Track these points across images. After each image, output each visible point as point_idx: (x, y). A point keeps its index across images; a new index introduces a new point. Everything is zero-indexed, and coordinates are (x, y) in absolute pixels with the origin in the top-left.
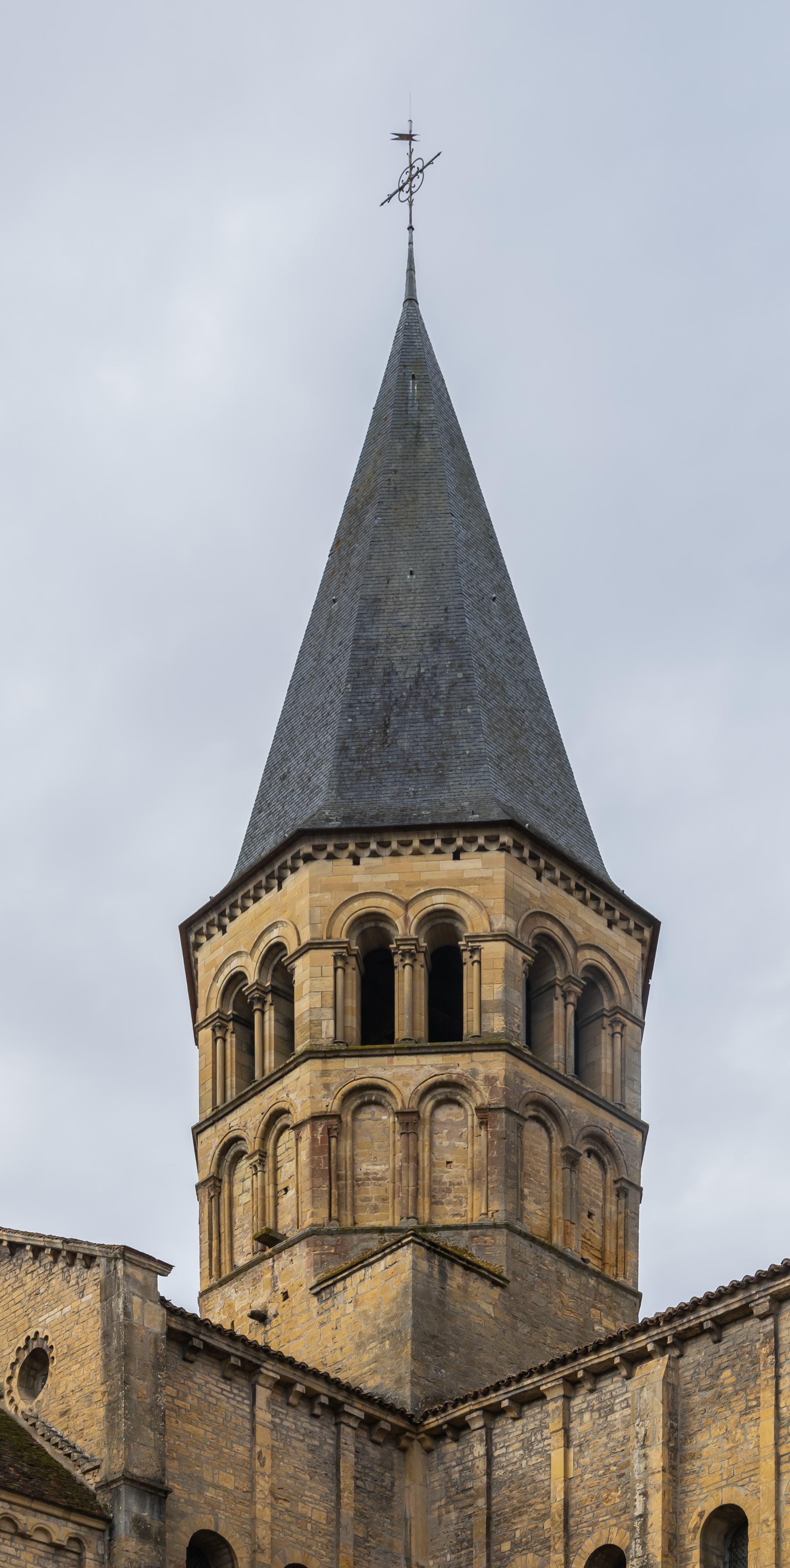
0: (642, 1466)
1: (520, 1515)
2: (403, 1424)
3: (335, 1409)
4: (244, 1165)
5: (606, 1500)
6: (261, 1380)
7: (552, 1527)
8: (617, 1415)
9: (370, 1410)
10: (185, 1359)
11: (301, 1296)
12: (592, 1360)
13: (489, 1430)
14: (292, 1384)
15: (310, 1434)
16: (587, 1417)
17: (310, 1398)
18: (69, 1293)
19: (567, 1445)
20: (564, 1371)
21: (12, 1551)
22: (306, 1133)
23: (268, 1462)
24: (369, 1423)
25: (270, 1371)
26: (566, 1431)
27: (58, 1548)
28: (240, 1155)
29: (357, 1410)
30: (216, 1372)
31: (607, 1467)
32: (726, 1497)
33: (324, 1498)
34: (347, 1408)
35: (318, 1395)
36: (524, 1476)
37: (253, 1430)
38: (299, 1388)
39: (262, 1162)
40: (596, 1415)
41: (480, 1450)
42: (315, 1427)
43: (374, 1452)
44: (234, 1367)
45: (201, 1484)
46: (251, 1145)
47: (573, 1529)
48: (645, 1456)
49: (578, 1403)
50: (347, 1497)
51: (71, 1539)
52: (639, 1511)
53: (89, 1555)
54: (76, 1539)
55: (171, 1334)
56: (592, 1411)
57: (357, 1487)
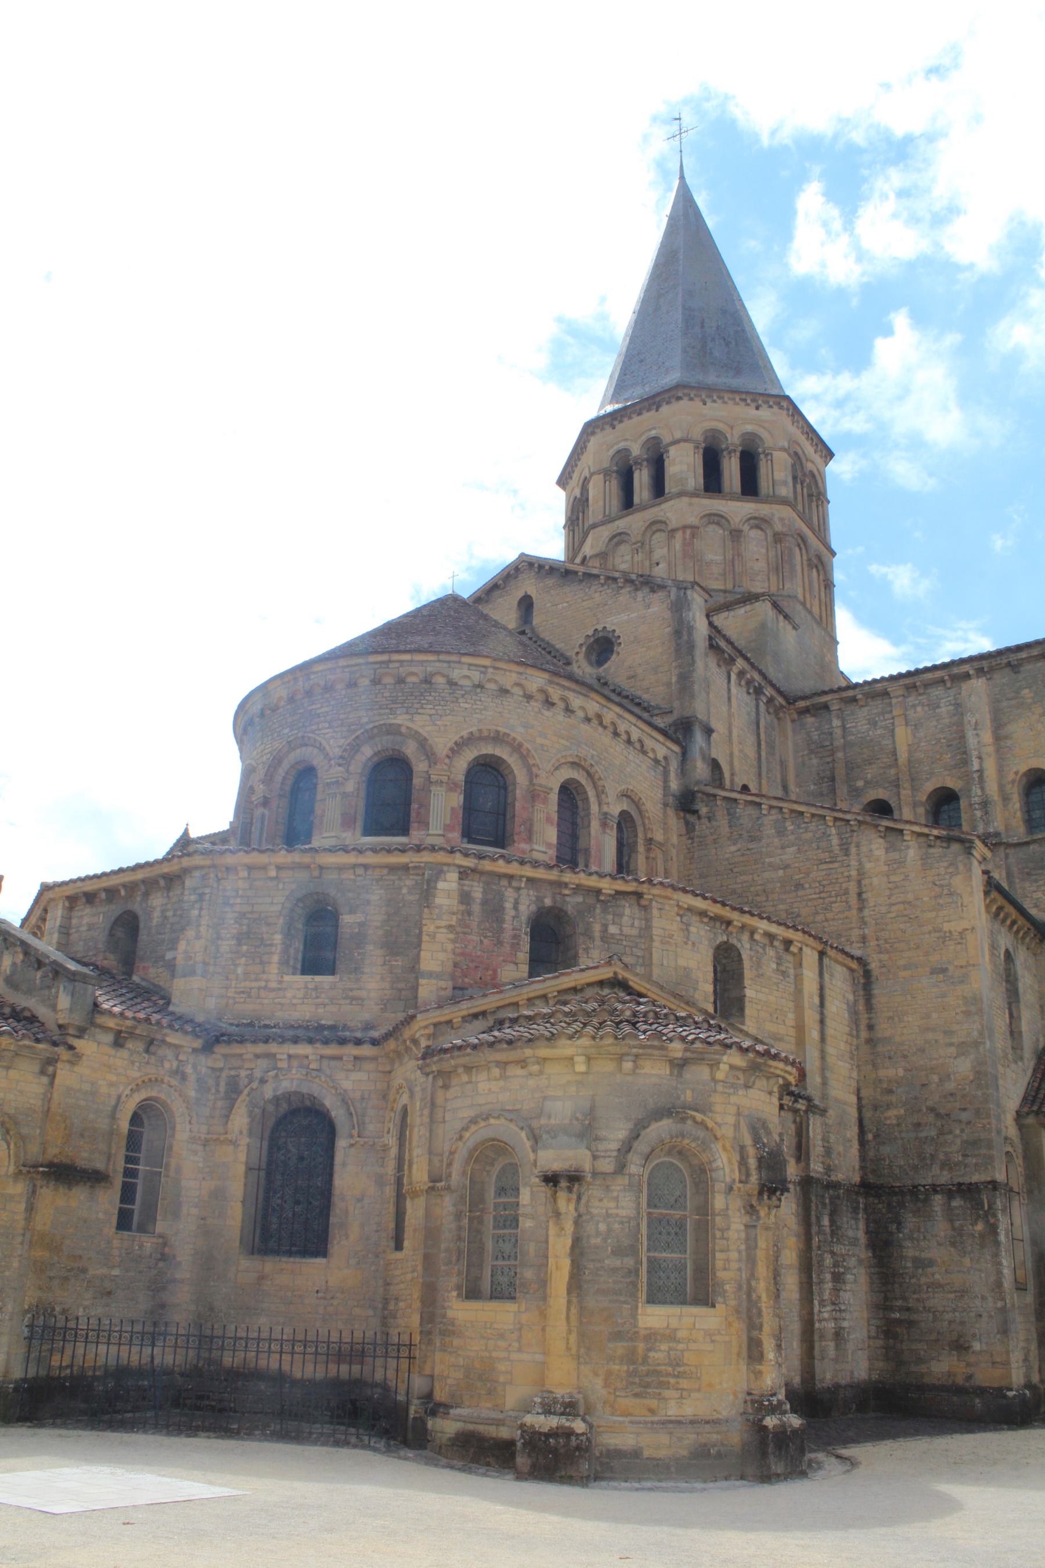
0: (976, 741)
1: (870, 764)
5: (940, 759)
8: (943, 709)
19: (907, 724)
31: (938, 740)
36: (871, 740)
38: (748, 676)
40: (926, 708)
44: (725, 659)
48: (977, 735)
52: (976, 766)
56: (923, 706)
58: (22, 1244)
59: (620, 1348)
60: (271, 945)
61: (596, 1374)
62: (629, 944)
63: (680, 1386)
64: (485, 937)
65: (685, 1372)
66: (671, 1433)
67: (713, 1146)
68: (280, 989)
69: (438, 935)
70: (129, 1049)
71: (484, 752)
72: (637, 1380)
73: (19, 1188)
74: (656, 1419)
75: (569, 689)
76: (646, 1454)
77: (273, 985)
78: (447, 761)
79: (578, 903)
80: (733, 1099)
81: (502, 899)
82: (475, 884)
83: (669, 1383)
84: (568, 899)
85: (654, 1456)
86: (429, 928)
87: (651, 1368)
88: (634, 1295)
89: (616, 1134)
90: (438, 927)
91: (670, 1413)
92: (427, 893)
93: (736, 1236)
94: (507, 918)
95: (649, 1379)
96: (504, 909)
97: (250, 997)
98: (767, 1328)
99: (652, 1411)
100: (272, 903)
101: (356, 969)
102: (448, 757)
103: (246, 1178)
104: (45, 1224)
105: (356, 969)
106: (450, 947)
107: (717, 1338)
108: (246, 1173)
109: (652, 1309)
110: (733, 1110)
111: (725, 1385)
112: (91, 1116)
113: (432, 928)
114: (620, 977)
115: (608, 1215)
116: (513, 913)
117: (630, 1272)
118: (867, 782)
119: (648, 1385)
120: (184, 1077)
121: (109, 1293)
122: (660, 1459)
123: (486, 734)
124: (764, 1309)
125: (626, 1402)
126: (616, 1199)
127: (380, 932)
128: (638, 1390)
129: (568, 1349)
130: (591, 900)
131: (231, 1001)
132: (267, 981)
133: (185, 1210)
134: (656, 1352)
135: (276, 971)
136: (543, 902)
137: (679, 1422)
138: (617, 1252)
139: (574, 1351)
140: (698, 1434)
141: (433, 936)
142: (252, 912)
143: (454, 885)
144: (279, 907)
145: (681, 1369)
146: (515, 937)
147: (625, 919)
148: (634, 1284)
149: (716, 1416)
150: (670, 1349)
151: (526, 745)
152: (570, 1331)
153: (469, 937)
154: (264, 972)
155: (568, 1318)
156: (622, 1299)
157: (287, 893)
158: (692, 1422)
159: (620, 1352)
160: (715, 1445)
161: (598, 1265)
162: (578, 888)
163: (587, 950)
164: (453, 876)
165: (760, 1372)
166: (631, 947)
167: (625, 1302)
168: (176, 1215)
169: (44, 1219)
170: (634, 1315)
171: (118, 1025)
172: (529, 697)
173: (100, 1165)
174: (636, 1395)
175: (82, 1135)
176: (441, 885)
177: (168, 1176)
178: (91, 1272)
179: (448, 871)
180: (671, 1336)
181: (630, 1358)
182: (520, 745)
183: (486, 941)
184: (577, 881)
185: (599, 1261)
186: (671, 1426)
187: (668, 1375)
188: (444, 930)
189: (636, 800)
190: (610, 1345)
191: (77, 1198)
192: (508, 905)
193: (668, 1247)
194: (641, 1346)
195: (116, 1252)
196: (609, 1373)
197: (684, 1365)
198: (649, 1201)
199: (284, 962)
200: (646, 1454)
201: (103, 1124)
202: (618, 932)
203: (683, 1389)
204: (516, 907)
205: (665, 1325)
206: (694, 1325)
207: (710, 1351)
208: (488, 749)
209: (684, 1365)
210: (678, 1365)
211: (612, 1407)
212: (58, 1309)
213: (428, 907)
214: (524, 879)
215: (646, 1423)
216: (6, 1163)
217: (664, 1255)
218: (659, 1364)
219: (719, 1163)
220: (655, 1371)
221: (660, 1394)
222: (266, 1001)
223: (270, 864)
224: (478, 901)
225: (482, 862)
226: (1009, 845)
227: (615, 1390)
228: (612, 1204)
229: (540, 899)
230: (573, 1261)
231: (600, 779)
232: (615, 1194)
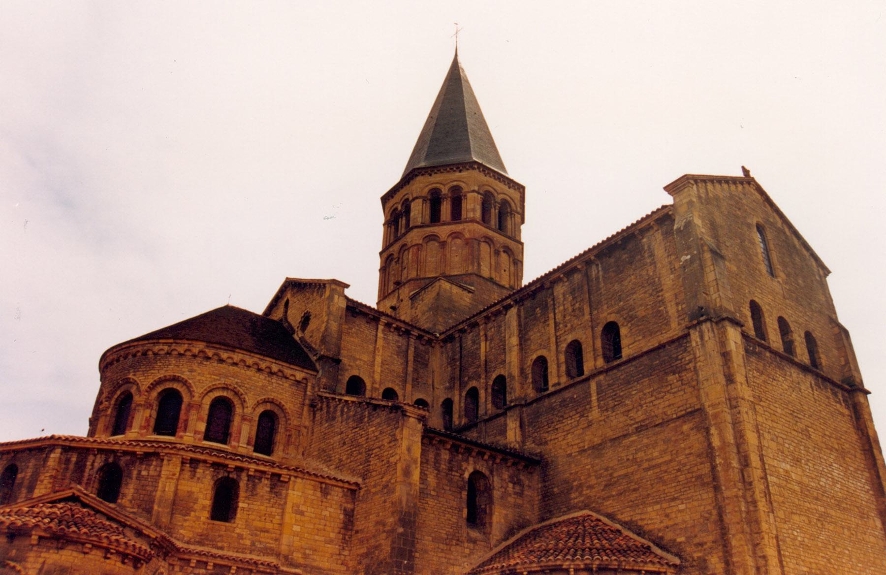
2: (433, 338)
3: (407, 333)
4: (393, 262)
6: (380, 323)
7: (481, 370)
9: (421, 333)
10: (353, 316)
11: (407, 303)
12: (493, 309)
13: (461, 338)
14: (392, 324)
15: (398, 341)
16: (493, 330)
17: (398, 329)
18: (318, 298)
20: (485, 314)
21: (280, 383)
22: (411, 250)
23: (381, 351)
24: (420, 337)
25: (383, 320)
26: (486, 336)
27: (298, 382)
28: (392, 260)
29: (415, 333)
30: (364, 321)
32: (540, 353)
33: (402, 364)
34: (412, 332)
35: (401, 328)
37: (376, 341)
39: (398, 260)
41: (458, 345)
42: (400, 339)
43: (421, 347)
44: (371, 319)
45: (355, 359)
46: (396, 256)
47: (488, 370)
49: (490, 325)
50: (411, 363)
51: (303, 379)
53: (309, 384)
54: (305, 379)
55: (348, 308)
57: (414, 360)
71: (168, 387)
75: (220, 349)
78: (146, 393)
80: (43, 555)
81: (86, 461)
92: (46, 460)
94: (87, 470)
102: (147, 391)
106: (50, 486)
110: (41, 560)
116: (90, 467)
118: (469, 378)
123: (168, 377)
127: (28, 481)
141: (42, 481)
147: (152, 467)
151: (190, 381)
163: (127, 484)
164: (59, 450)
172: (194, 356)
176: (52, 455)
182: (186, 381)
189: (278, 403)
204: (92, 465)
208: (169, 385)
224: (73, 462)
226: (522, 406)
229: (106, 460)
231: (242, 394)
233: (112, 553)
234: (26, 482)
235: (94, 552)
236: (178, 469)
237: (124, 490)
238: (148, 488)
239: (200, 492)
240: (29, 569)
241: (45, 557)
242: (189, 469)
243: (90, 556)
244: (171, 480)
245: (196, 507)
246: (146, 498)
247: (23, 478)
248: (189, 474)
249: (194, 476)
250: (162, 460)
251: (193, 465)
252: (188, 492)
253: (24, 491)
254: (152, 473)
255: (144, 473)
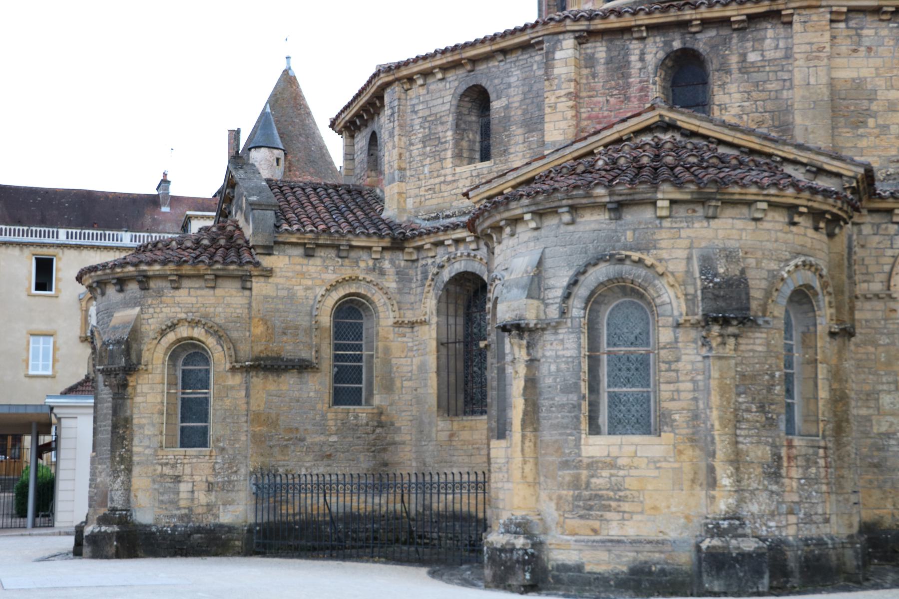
58: (246, 422)
59: (567, 475)
60: (446, 142)
61: (551, 499)
62: (773, 68)
63: (622, 509)
64: (612, 96)
65: (626, 497)
66: (609, 551)
67: (657, 282)
68: (454, 181)
69: (559, 105)
70: (321, 257)
72: (581, 503)
73: (237, 380)
74: (598, 538)
76: (588, 568)
77: (449, 178)
79: (712, 38)
80: (684, 233)
81: (627, 54)
82: (599, 44)
83: (610, 506)
84: (699, 36)
85: (595, 570)
86: (551, 99)
87: (593, 493)
88: (577, 428)
89: (558, 281)
90: (558, 97)
91: (612, 533)
92: (548, 64)
93: (689, 367)
95: (591, 503)
96: (629, 62)
97: (435, 193)
98: (720, 455)
99: (595, 531)
100: (443, 103)
101: (505, 151)
103: (438, 351)
104: (259, 406)
105: (505, 151)
107: (664, 465)
108: (438, 347)
109: (594, 439)
110: (685, 243)
111: (673, 509)
112: (291, 316)
113: (553, 99)
114: (667, 119)
115: (557, 357)
116: (639, 65)
117: (574, 407)
119: (591, 508)
120: (382, 273)
121: (329, 456)
122: (600, 574)
124: (717, 438)
125: (574, 523)
126: (562, 340)
127: (519, 112)
128: (582, 512)
129: (524, 477)
130: (725, 32)
131: (423, 199)
132: (445, 176)
133: (398, 384)
134: (598, 478)
135: (451, 165)
136: (671, 46)
137: (619, 542)
138: (566, 390)
139: (530, 479)
140: (637, 552)
141: (554, 107)
142: (430, 116)
143: (570, 52)
144: (447, 106)
145: (622, 494)
146: (642, 89)
147: (768, 41)
148: (577, 418)
149: (661, 537)
150: (612, 475)
152: (525, 462)
153: (595, 99)
154: (442, 168)
155: (523, 450)
156: (569, 431)
157: (452, 91)
158: (633, 542)
159: (568, 478)
160: (658, 563)
161: (551, 402)
162: (706, 23)
163: (723, 86)
164: (569, 42)
165: (714, 497)
166: (776, 72)
167: (571, 435)
168: (389, 387)
169: (259, 400)
170: (578, 445)
171: (299, 239)
173: (306, 354)
174: (581, 517)
175: (284, 333)
176: (558, 55)
177: (377, 358)
178: (309, 440)
179: (564, 39)
180: (612, 464)
181: (575, 484)
183: (612, 100)
184: (698, 16)
185: (553, 399)
186: (610, 544)
187: (610, 499)
188: (564, 99)
190: (560, 473)
191: (288, 383)
192: (634, 58)
193: (628, 382)
194: (584, 473)
195: (331, 423)
196: (560, 498)
197: (626, 489)
198: (608, 340)
199: (458, 156)
200: (588, 568)
201: (304, 322)
202: (760, 58)
203: (624, 512)
204: (642, 59)
205: (606, 454)
206: (636, 452)
207: (655, 477)
209: (626, 489)
210: (619, 490)
211: (562, 527)
212: (281, 470)
213: (548, 79)
214: (643, 28)
215: (588, 541)
216: (223, 362)
217: (625, 389)
218: (600, 489)
219: (665, 298)
220: (596, 495)
221: (602, 516)
222: (446, 194)
223: (434, 68)
224: (602, 61)
225: (592, 23)
227: (564, 511)
228: (560, 347)
230: (526, 400)
232: (561, 337)
233: (801, 214)
234: (517, 114)
235: (771, 215)
236: (827, 36)
237: (719, 97)
238: (769, 86)
239: (878, 75)
240: (667, 261)
241: (689, 237)
242: (846, 33)
243: (766, 225)
244: (816, 62)
245: (874, 107)
246: (770, 106)
247: (507, 108)
248: (849, 41)
249: (859, 45)
250: (790, 23)
251: (852, 24)
252: (853, 80)
253: (517, 132)
254: (770, 55)
255: (753, 57)
